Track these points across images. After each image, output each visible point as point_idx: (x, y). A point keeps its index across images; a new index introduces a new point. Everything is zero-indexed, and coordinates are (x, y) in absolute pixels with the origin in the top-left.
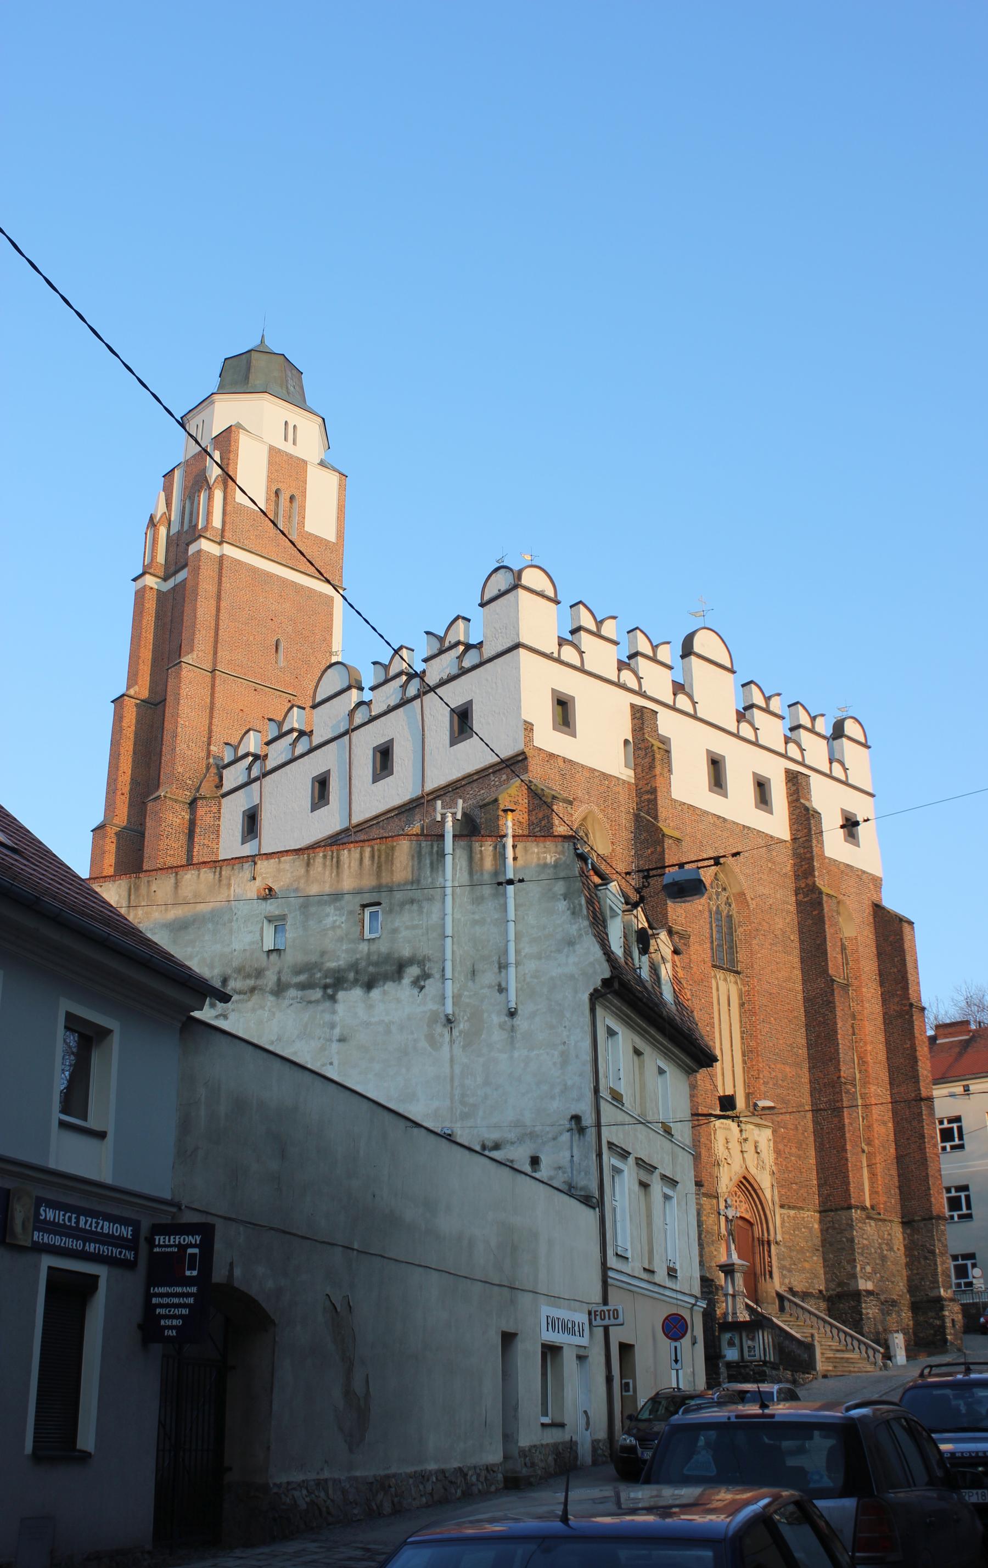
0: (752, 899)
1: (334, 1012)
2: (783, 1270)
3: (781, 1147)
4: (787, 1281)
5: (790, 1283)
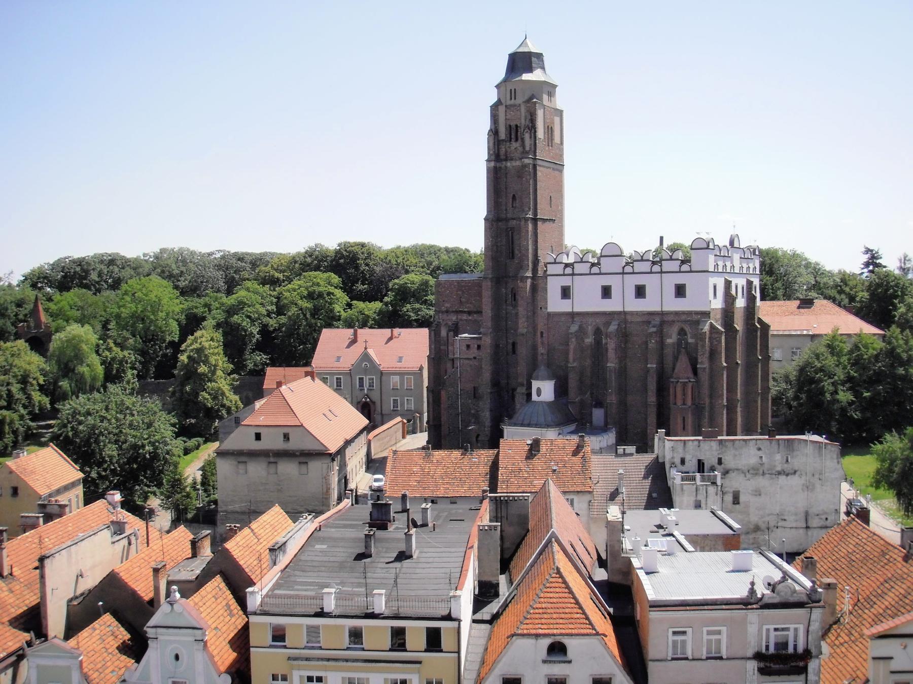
1: (778, 481)
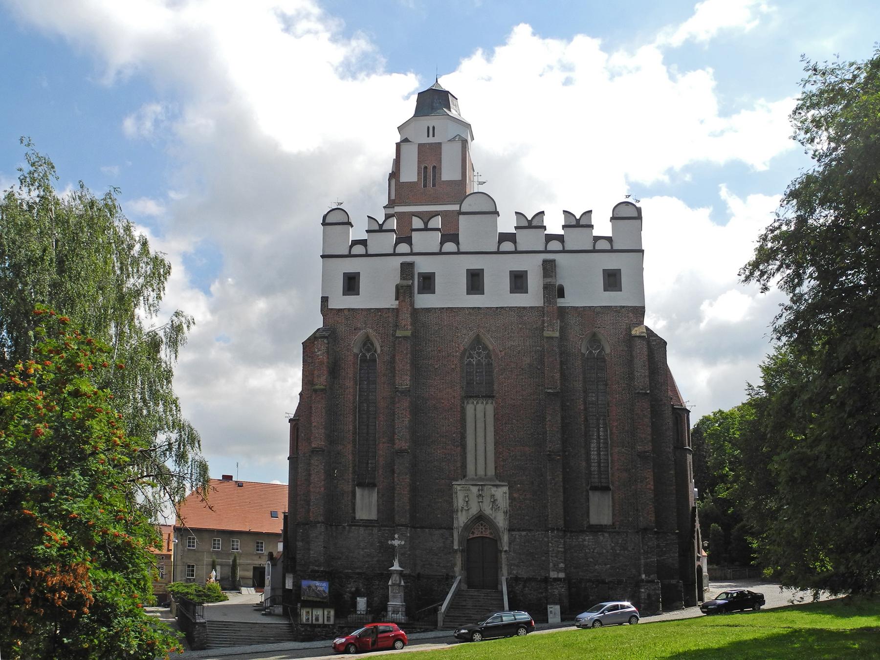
0: (501, 351)
2: (512, 566)
3: (515, 495)
4: (515, 572)
5: (517, 573)
